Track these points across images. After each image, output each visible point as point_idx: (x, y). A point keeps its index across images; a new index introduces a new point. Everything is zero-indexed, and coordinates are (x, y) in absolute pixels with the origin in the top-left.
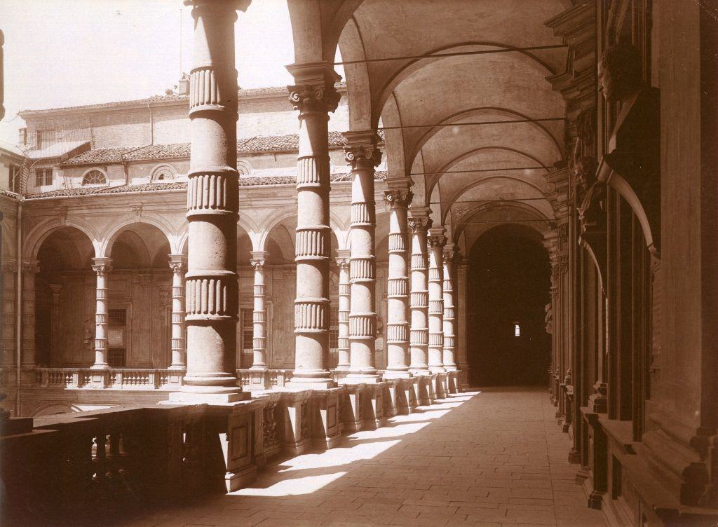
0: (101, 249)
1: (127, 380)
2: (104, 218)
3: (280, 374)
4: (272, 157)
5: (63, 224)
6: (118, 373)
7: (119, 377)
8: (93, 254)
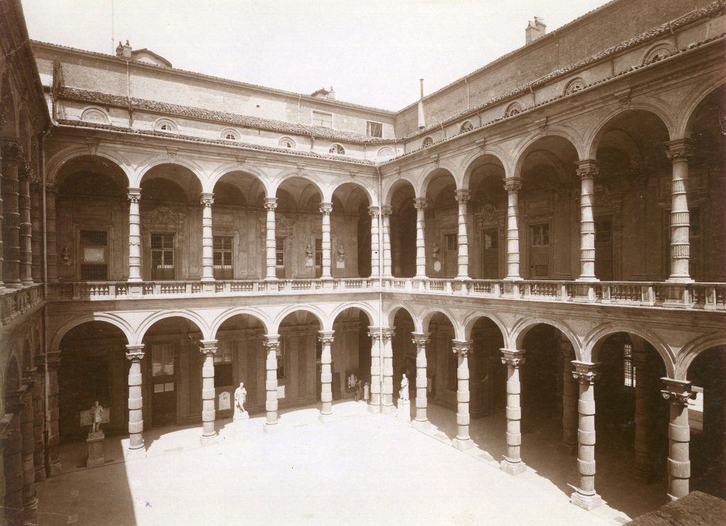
0: (271, 193)
1: (165, 291)
2: (139, 155)
3: (290, 282)
4: (257, 131)
5: (92, 154)
6: (112, 285)
7: (158, 287)
8: (263, 194)
